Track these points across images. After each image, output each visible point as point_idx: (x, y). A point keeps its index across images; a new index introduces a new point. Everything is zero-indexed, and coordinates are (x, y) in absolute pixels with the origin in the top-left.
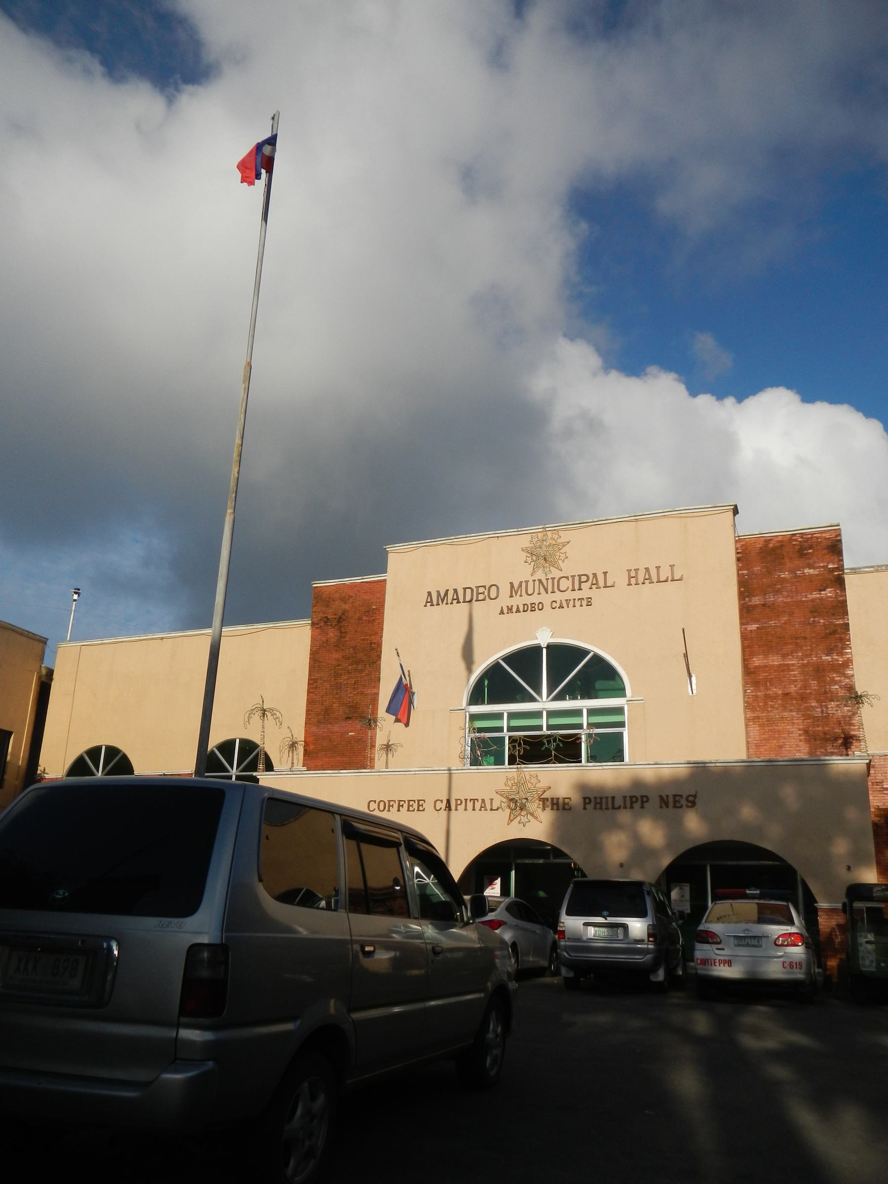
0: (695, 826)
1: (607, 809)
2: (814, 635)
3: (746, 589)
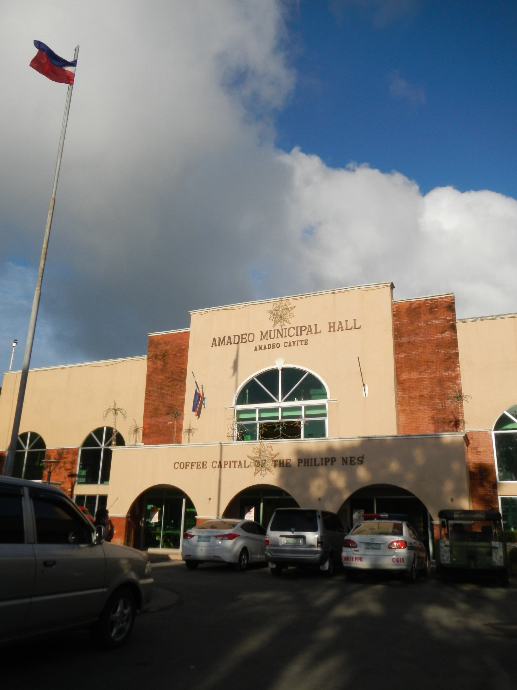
0: (363, 475)
1: (312, 465)
2: (438, 360)
3: (398, 333)
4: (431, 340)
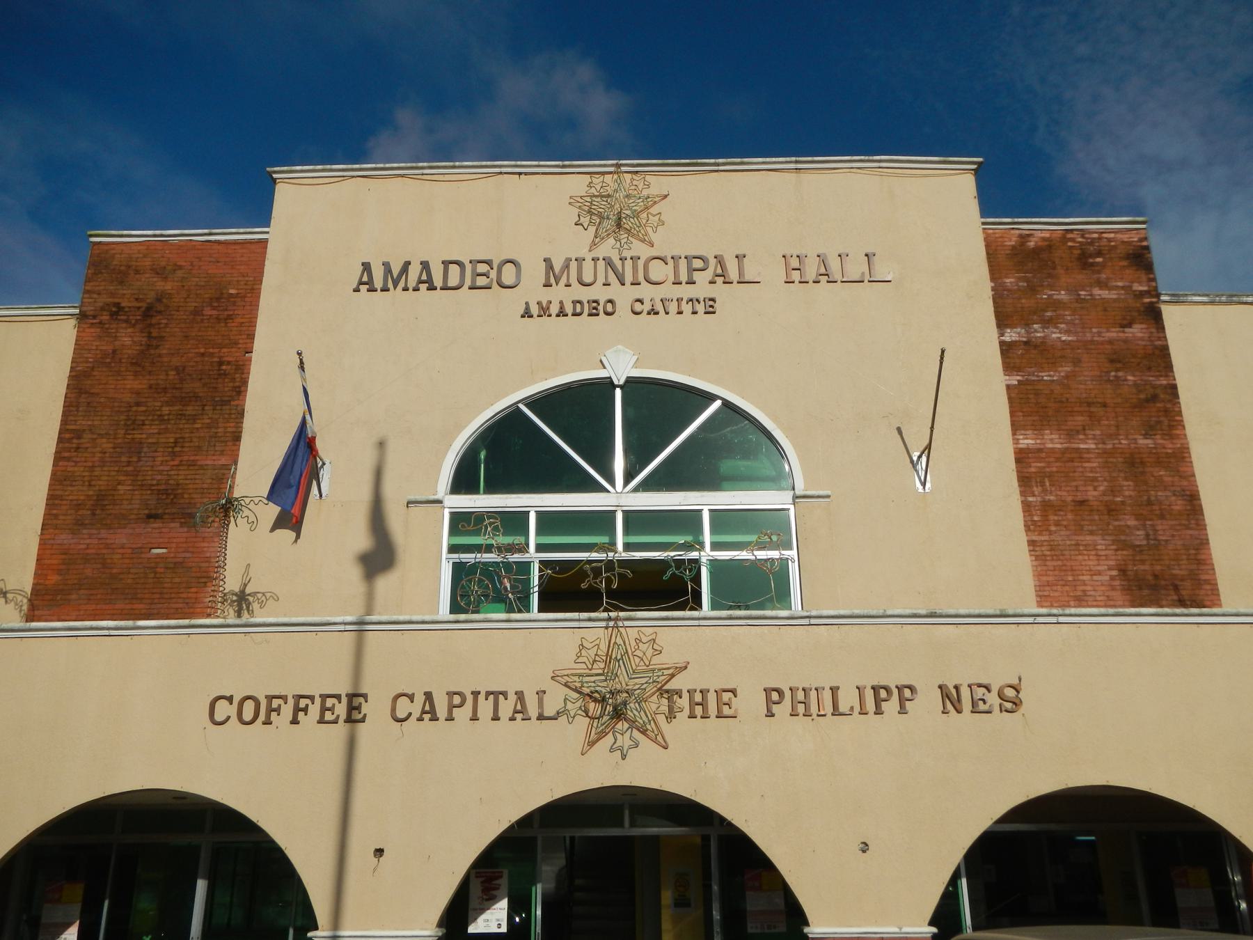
2: (1120, 400)
4: (1092, 342)
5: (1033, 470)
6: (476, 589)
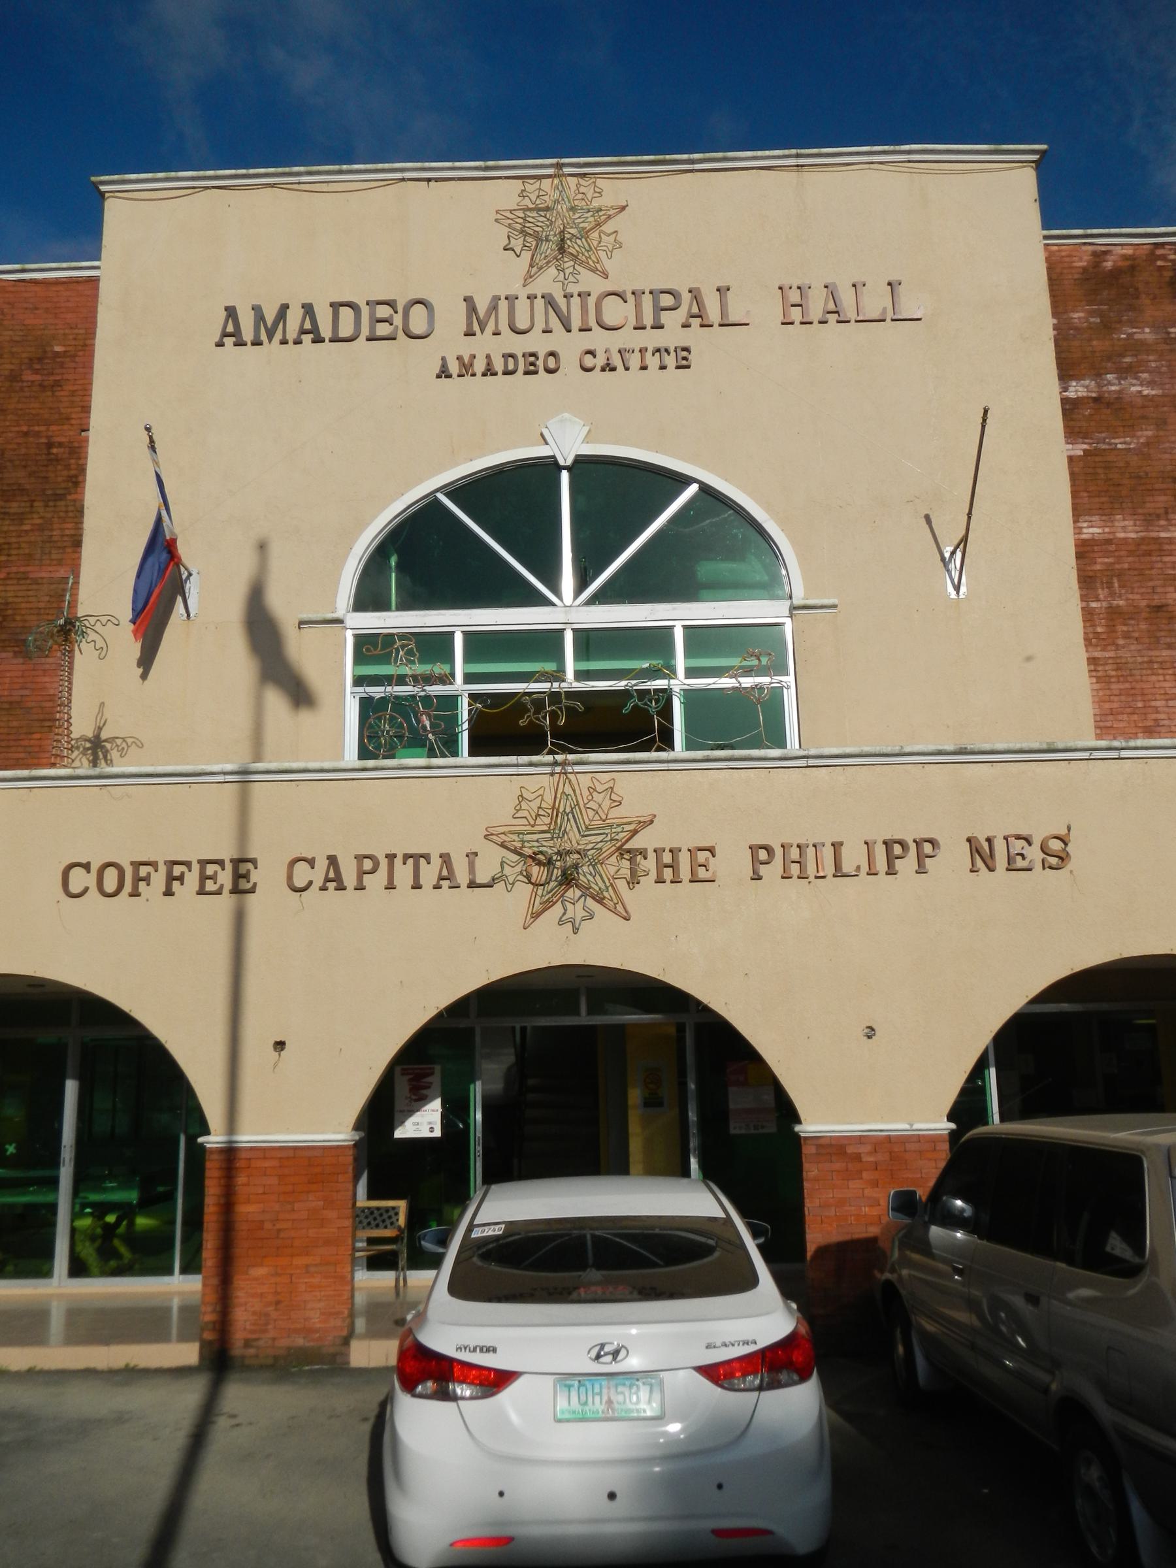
5: (1098, 567)
6: (391, 729)
